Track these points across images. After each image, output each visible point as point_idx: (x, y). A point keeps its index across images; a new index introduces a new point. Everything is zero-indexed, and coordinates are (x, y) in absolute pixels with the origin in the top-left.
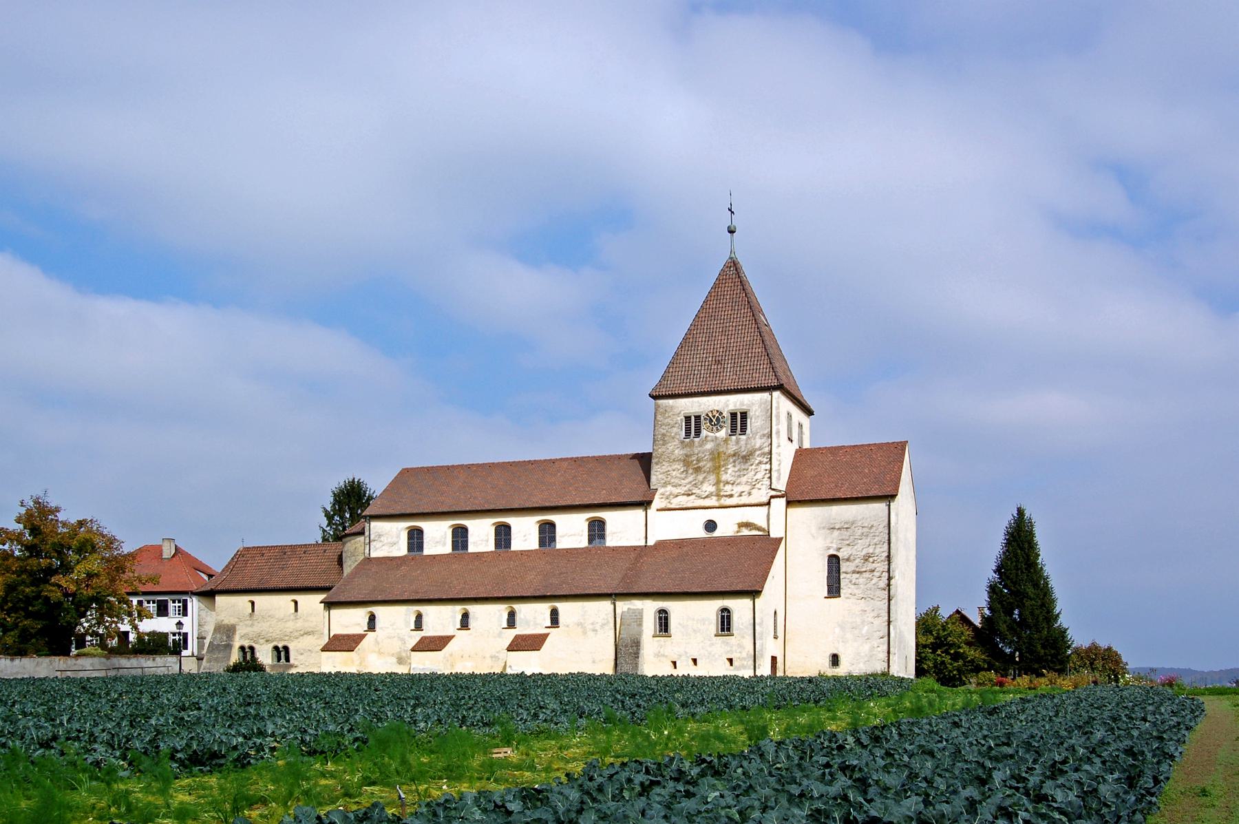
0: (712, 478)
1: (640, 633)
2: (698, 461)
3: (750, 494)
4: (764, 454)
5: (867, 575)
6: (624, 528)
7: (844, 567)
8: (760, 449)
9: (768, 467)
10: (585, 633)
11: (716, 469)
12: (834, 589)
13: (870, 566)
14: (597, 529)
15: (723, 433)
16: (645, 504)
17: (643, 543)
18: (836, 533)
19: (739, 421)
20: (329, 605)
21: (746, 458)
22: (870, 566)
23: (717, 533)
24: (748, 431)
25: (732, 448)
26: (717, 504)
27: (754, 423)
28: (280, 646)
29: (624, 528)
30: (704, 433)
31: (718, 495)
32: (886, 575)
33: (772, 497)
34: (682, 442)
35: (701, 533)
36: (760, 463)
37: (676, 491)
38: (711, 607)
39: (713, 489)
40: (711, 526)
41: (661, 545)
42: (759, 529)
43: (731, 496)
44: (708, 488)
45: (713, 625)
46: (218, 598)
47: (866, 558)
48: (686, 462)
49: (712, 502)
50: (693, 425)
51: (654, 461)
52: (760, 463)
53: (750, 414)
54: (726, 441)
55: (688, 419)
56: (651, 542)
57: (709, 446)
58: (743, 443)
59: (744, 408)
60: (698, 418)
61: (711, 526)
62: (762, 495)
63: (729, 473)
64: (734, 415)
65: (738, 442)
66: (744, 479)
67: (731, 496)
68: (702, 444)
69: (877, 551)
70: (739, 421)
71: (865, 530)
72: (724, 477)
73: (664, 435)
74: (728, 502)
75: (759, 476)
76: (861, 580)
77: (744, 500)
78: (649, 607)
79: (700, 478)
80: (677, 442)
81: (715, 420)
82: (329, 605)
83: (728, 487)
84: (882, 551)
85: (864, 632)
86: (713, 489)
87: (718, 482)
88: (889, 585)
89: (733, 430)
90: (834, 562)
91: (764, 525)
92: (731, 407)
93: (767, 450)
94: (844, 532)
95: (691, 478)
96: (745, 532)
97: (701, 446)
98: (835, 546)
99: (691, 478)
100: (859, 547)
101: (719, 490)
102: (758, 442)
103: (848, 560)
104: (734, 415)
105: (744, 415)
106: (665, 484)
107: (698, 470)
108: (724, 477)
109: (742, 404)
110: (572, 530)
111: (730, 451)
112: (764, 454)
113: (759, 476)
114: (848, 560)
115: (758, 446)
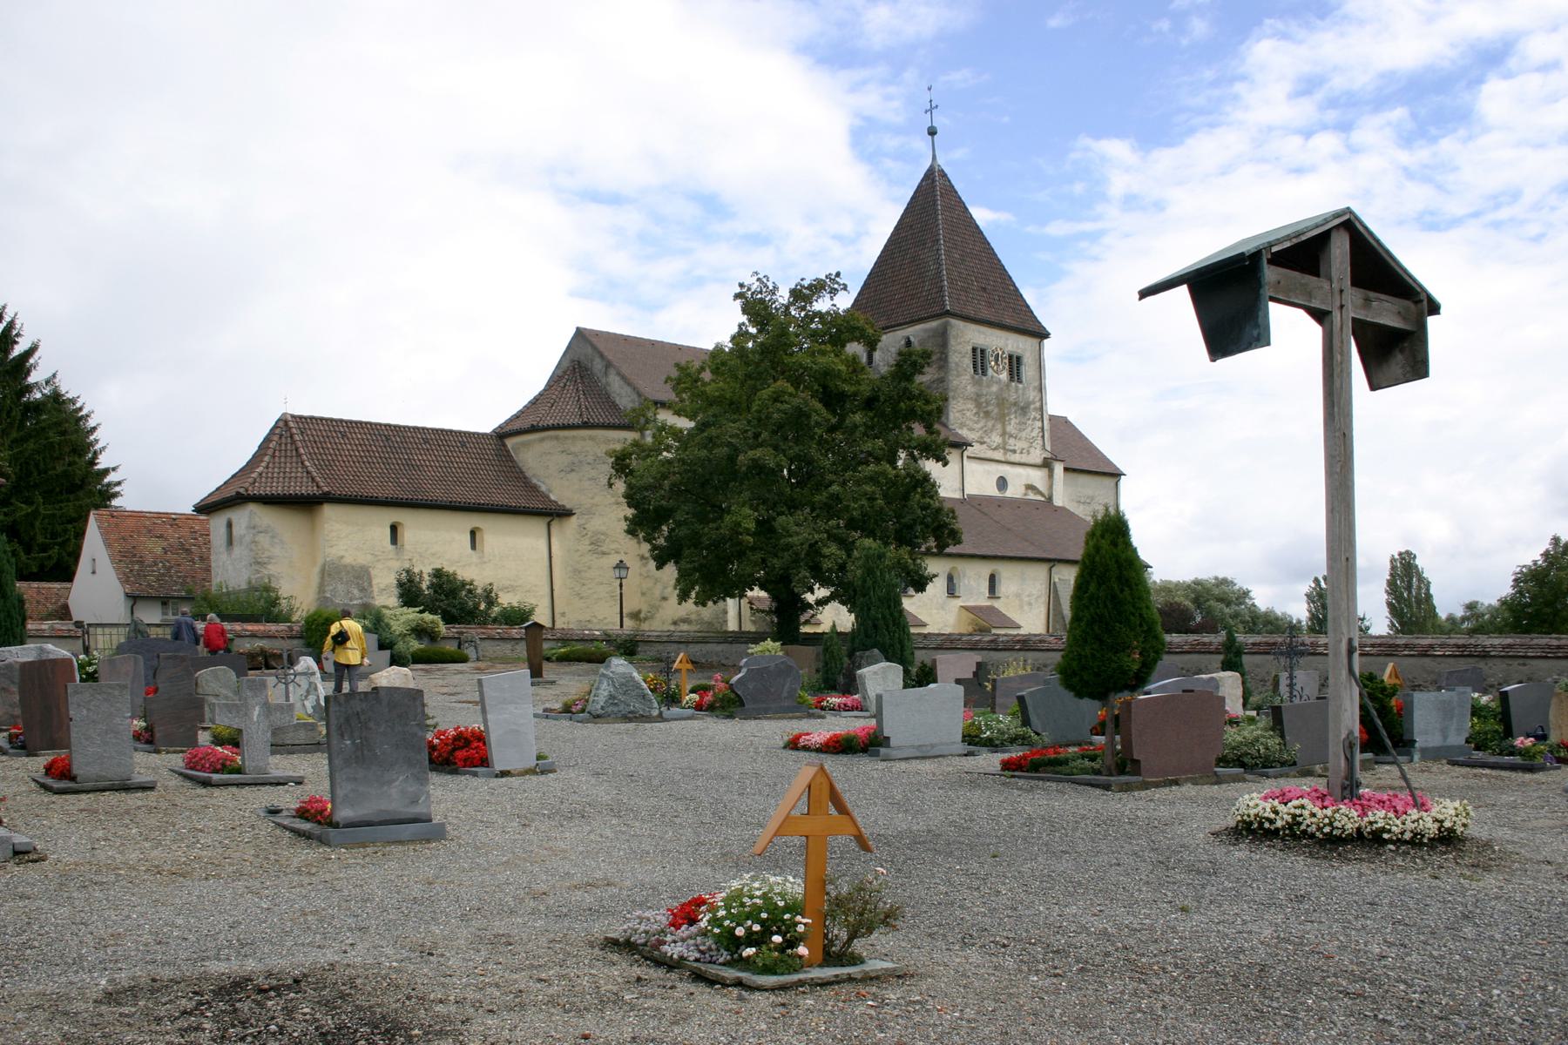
0: (999, 426)
2: (988, 404)
9: (1039, 424)
10: (1021, 607)
11: (1002, 418)
19: (1015, 363)
21: (1024, 410)
27: (1028, 371)
30: (990, 372)
31: (1006, 450)
35: (992, 491)
40: (1002, 483)
43: (1014, 451)
44: (996, 439)
48: (977, 399)
49: (998, 455)
55: (974, 350)
57: (995, 388)
60: (983, 351)
61: (1002, 483)
65: (1017, 390)
66: (1024, 434)
67: (1014, 451)
72: (1010, 429)
74: (1016, 458)
79: (990, 424)
83: (1012, 441)
87: (1004, 434)
89: (1012, 379)
91: (1046, 493)
96: (1032, 496)
101: (1005, 443)
102: (1032, 395)
105: (1019, 359)
106: (962, 425)
108: (1010, 429)
111: (1012, 399)
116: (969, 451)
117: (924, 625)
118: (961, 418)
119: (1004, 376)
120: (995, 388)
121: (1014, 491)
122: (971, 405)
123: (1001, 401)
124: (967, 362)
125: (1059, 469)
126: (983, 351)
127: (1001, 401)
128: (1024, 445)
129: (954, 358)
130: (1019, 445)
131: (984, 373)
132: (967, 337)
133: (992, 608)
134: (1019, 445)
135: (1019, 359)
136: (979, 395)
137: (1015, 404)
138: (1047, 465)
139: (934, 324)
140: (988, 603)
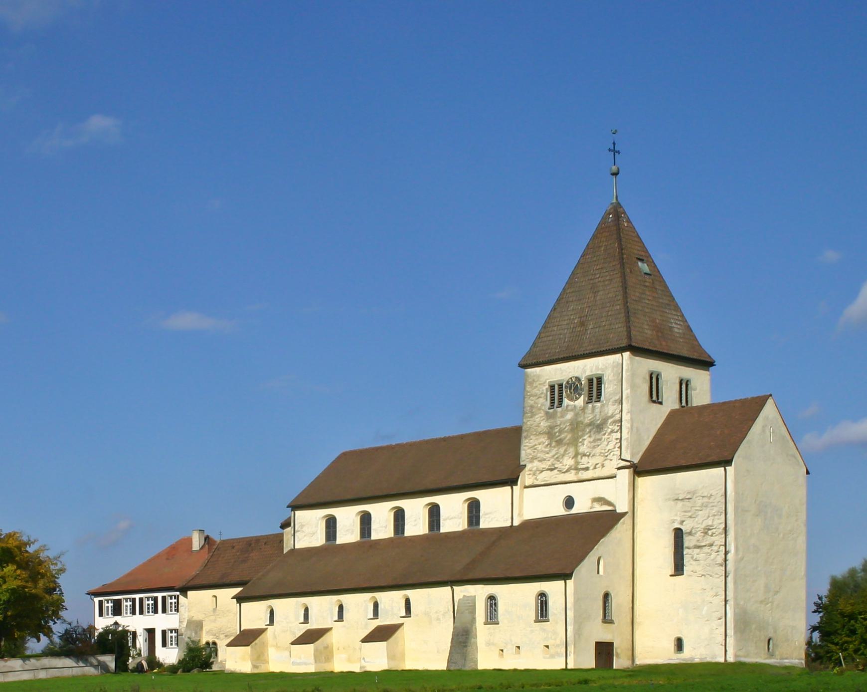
0: (572, 450)
1: (474, 620)
2: (561, 432)
3: (603, 466)
4: (615, 422)
5: (706, 549)
6: (499, 508)
7: (688, 541)
8: (612, 416)
9: (619, 436)
11: (575, 442)
12: (679, 568)
13: (709, 540)
15: (580, 402)
16: (512, 482)
17: (509, 524)
18: (680, 504)
19: (594, 387)
20: (240, 599)
21: (599, 427)
22: (709, 540)
23: (575, 510)
24: (602, 398)
25: (588, 417)
26: (575, 479)
27: (608, 389)
28: (211, 641)
29: (499, 508)
30: (566, 401)
32: (723, 548)
33: (619, 469)
34: (547, 413)
35: (559, 510)
36: (612, 432)
37: (542, 466)
38: (528, 591)
40: (569, 502)
41: (528, 525)
42: (609, 503)
43: (587, 469)
44: (568, 462)
45: (531, 612)
46: (189, 593)
47: (706, 531)
48: (550, 433)
51: (524, 434)
52: (612, 432)
53: (605, 379)
54: (583, 409)
55: (552, 387)
56: (516, 523)
57: (569, 416)
58: (597, 411)
60: (561, 386)
61: (569, 502)
65: (594, 408)
67: (587, 469)
69: (716, 522)
70: (594, 387)
71: (705, 500)
72: (583, 449)
73: (532, 407)
75: (611, 446)
76: (702, 556)
77: (598, 473)
79: (562, 450)
80: (542, 414)
81: (573, 387)
82: (240, 599)
83: (585, 460)
84: (719, 522)
85: (704, 613)
88: (726, 560)
89: (590, 400)
90: (679, 535)
92: (588, 373)
93: (618, 417)
94: (686, 503)
95: (553, 452)
96: (598, 508)
97: (562, 417)
98: (679, 519)
99: (553, 452)
100: (699, 519)
101: (577, 463)
102: (612, 409)
103: (690, 533)
104: (590, 381)
105: (600, 380)
106: (532, 460)
107: (560, 442)
108: (583, 449)
109: (597, 368)
111: (587, 421)
112: (615, 422)
113: (611, 446)
114: (690, 533)
115: (610, 414)
122: (544, 439)
127: (576, 427)
128: (598, 460)
132: (542, 380)
136: (552, 428)
137: (591, 424)
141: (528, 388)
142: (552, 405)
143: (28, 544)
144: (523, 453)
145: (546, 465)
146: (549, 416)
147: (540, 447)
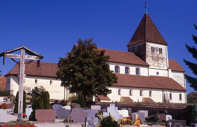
6: (144, 72)
11: (157, 61)
14: (137, 70)
16: (147, 66)
19: (161, 50)
21: (163, 59)
23: (160, 75)
29: (144, 72)
30: (155, 52)
35: (155, 75)
39: (157, 65)
40: (158, 73)
44: (156, 64)
48: (152, 57)
49: (157, 68)
50: (153, 49)
53: (163, 49)
57: (156, 55)
58: (162, 55)
59: (162, 48)
60: (154, 48)
61: (158, 73)
62: (166, 68)
63: (160, 62)
64: (160, 49)
68: (155, 54)
70: (161, 50)
74: (160, 68)
78: (168, 93)
86: (157, 65)
89: (160, 53)
95: (153, 62)
102: (164, 56)
105: (161, 49)
107: (154, 60)
110: (133, 70)
113: (165, 63)
116: (149, 67)
117: (133, 101)
118: (149, 60)
119: (158, 52)
120: (156, 55)
121: (160, 75)
122: (151, 58)
123: (158, 57)
124: (150, 50)
125: (170, 70)
126: (154, 48)
129: (147, 49)
130: (161, 66)
131: (154, 52)
133: (150, 98)
134: (161, 66)
135: (161, 49)
137: (161, 58)
138: (168, 70)
139: (143, 43)
140: (149, 97)
141: (147, 46)
142: (152, 52)
143: (189, 68)
144: (147, 60)
145: (152, 64)
146: (152, 54)
147: (150, 60)
